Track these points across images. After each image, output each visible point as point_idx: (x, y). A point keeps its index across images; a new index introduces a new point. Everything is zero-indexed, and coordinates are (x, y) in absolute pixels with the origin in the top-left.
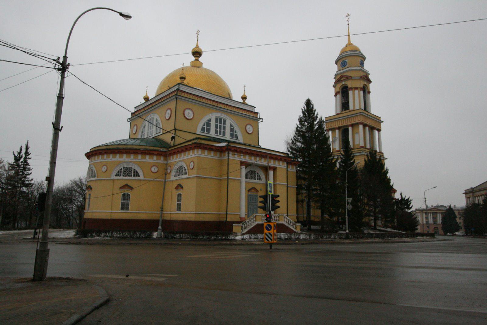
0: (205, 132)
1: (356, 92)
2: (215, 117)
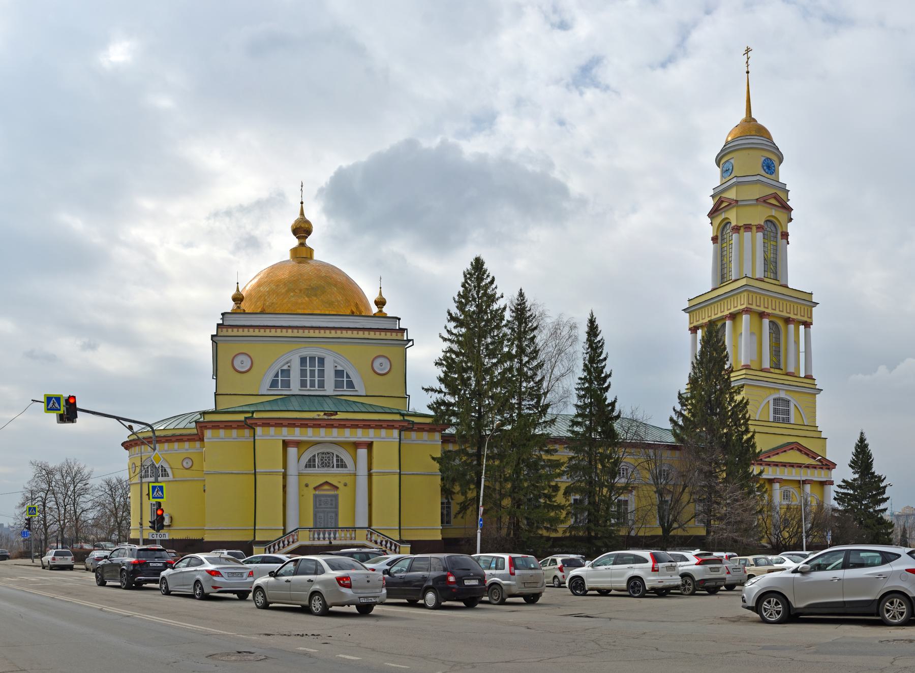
0: (280, 388)
1: (747, 235)
2: (300, 356)
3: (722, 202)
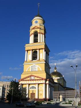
1: (41, 35)
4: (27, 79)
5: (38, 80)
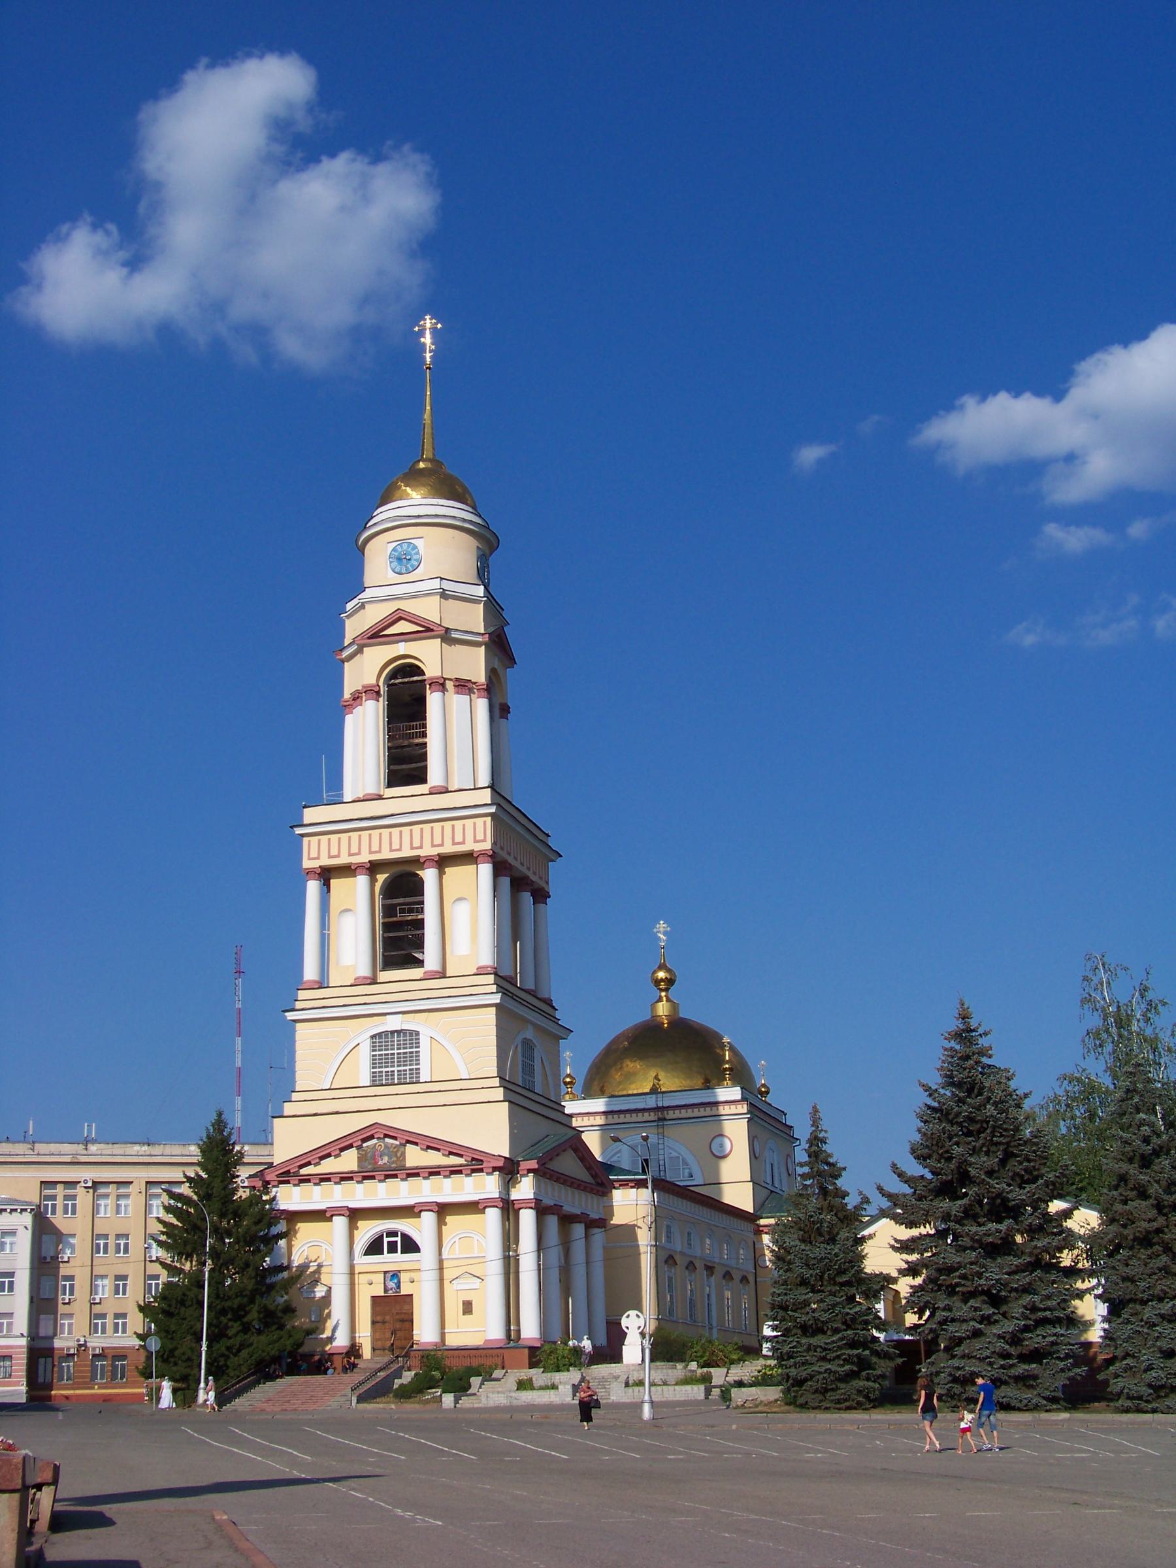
3: (400, 619)
4: (328, 1166)
5: (434, 1172)
